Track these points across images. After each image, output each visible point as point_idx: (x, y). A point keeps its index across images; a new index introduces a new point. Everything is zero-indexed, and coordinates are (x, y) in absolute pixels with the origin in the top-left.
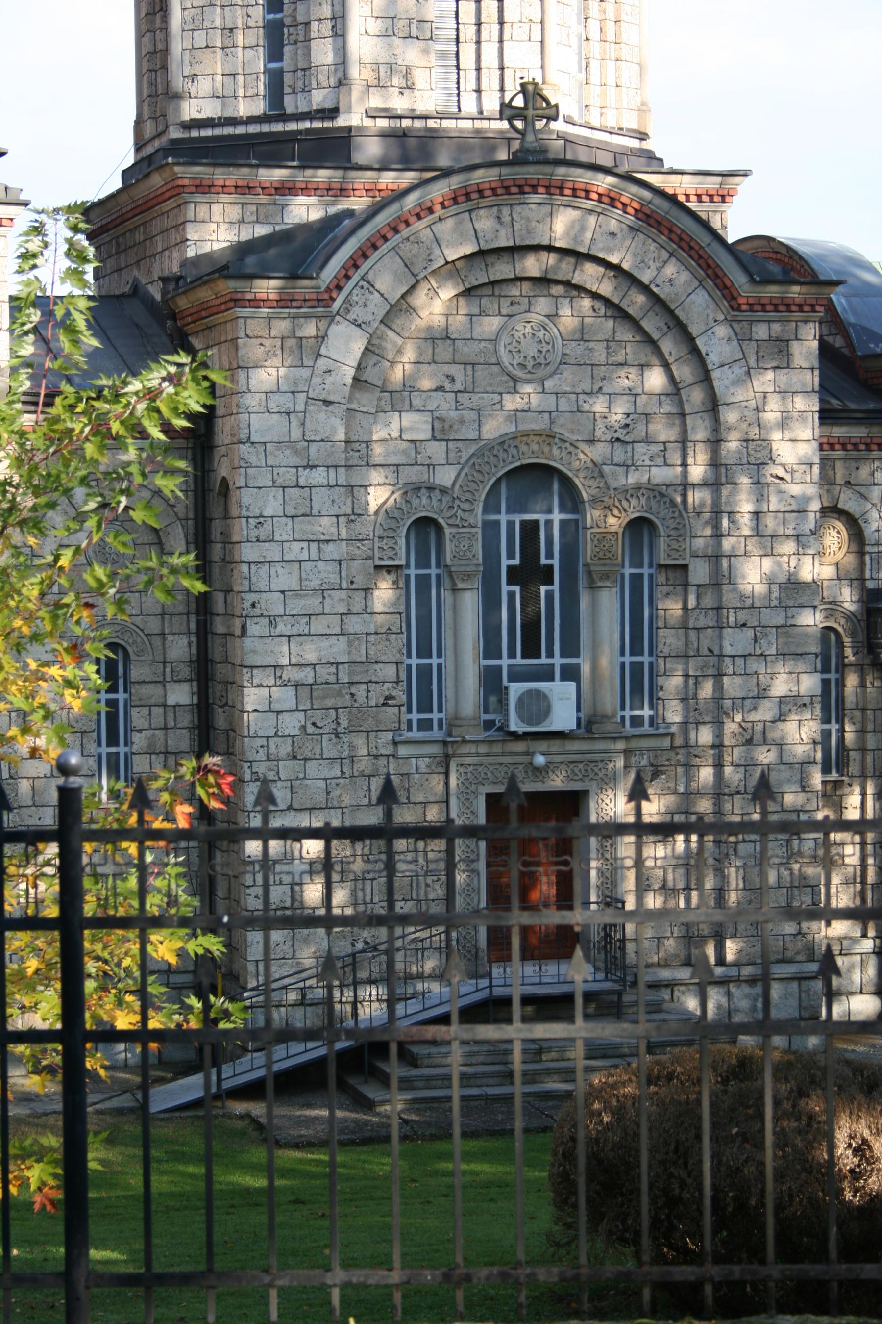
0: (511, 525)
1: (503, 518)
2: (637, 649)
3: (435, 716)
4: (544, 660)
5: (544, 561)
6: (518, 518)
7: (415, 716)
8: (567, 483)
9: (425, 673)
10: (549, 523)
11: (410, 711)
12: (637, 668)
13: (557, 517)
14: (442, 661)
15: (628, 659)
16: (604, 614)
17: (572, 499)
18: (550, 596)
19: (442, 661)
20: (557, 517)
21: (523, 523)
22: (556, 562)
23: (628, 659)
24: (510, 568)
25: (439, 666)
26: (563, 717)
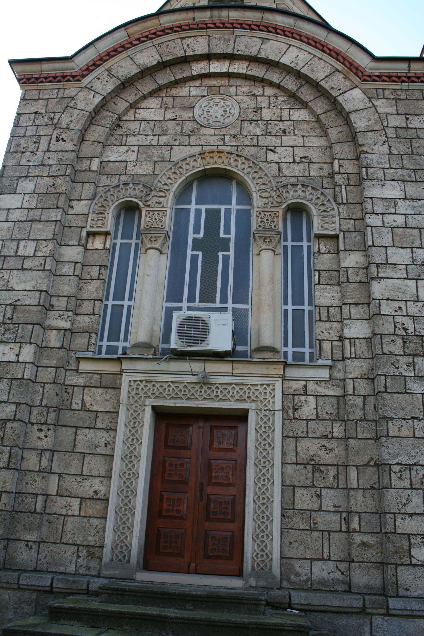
0: (198, 212)
1: (193, 207)
2: (298, 299)
3: (121, 344)
4: (218, 304)
5: (222, 235)
6: (204, 208)
7: (105, 344)
8: (242, 185)
9: (117, 310)
10: (228, 212)
11: (102, 340)
12: (298, 316)
13: (234, 207)
14: (131, 303)
15: (290, 307)
16: (267, 267)
17: (245, 196)
18: (226, 259)
19: (131, 303)
20: (234, 207)
21: (207, 211)
22: (232, 236)
23: (290, 307)
24: (194, 239)
25: (129, 307)
26: (220, 338)
